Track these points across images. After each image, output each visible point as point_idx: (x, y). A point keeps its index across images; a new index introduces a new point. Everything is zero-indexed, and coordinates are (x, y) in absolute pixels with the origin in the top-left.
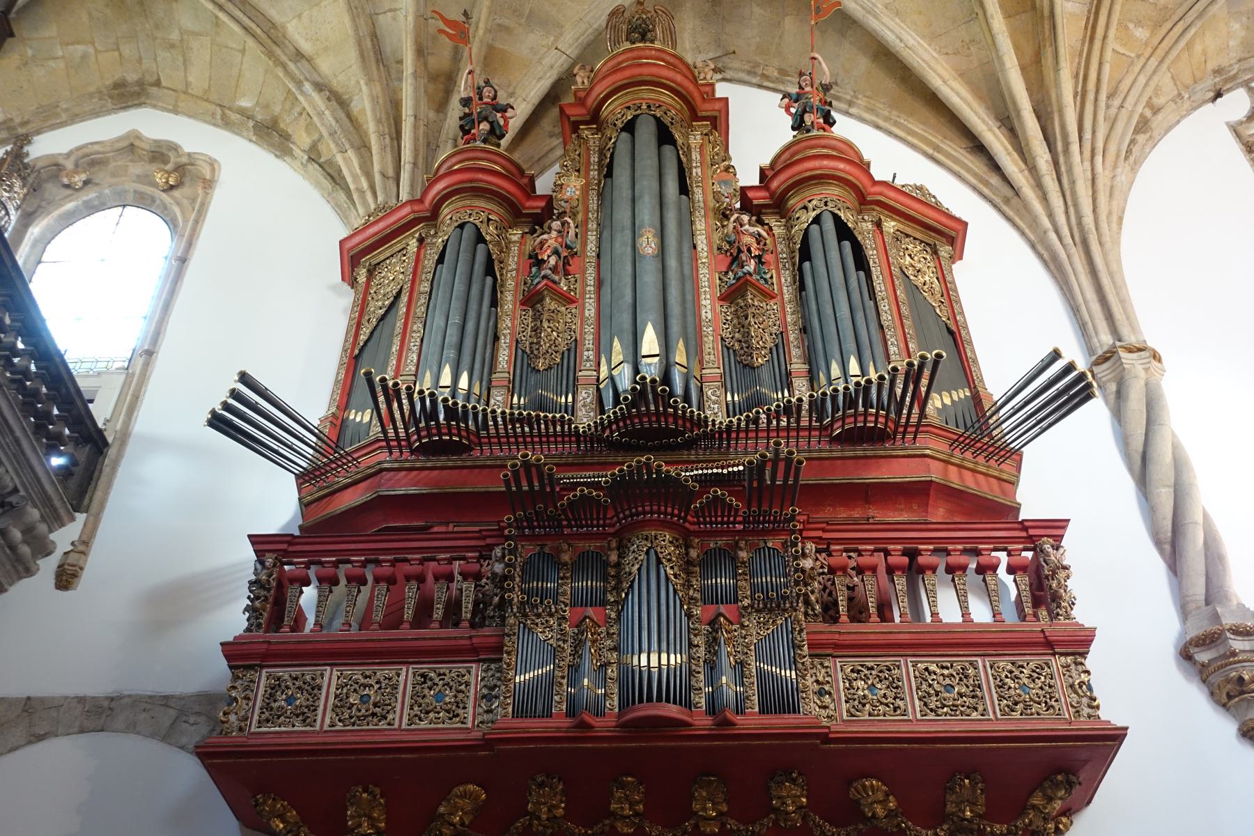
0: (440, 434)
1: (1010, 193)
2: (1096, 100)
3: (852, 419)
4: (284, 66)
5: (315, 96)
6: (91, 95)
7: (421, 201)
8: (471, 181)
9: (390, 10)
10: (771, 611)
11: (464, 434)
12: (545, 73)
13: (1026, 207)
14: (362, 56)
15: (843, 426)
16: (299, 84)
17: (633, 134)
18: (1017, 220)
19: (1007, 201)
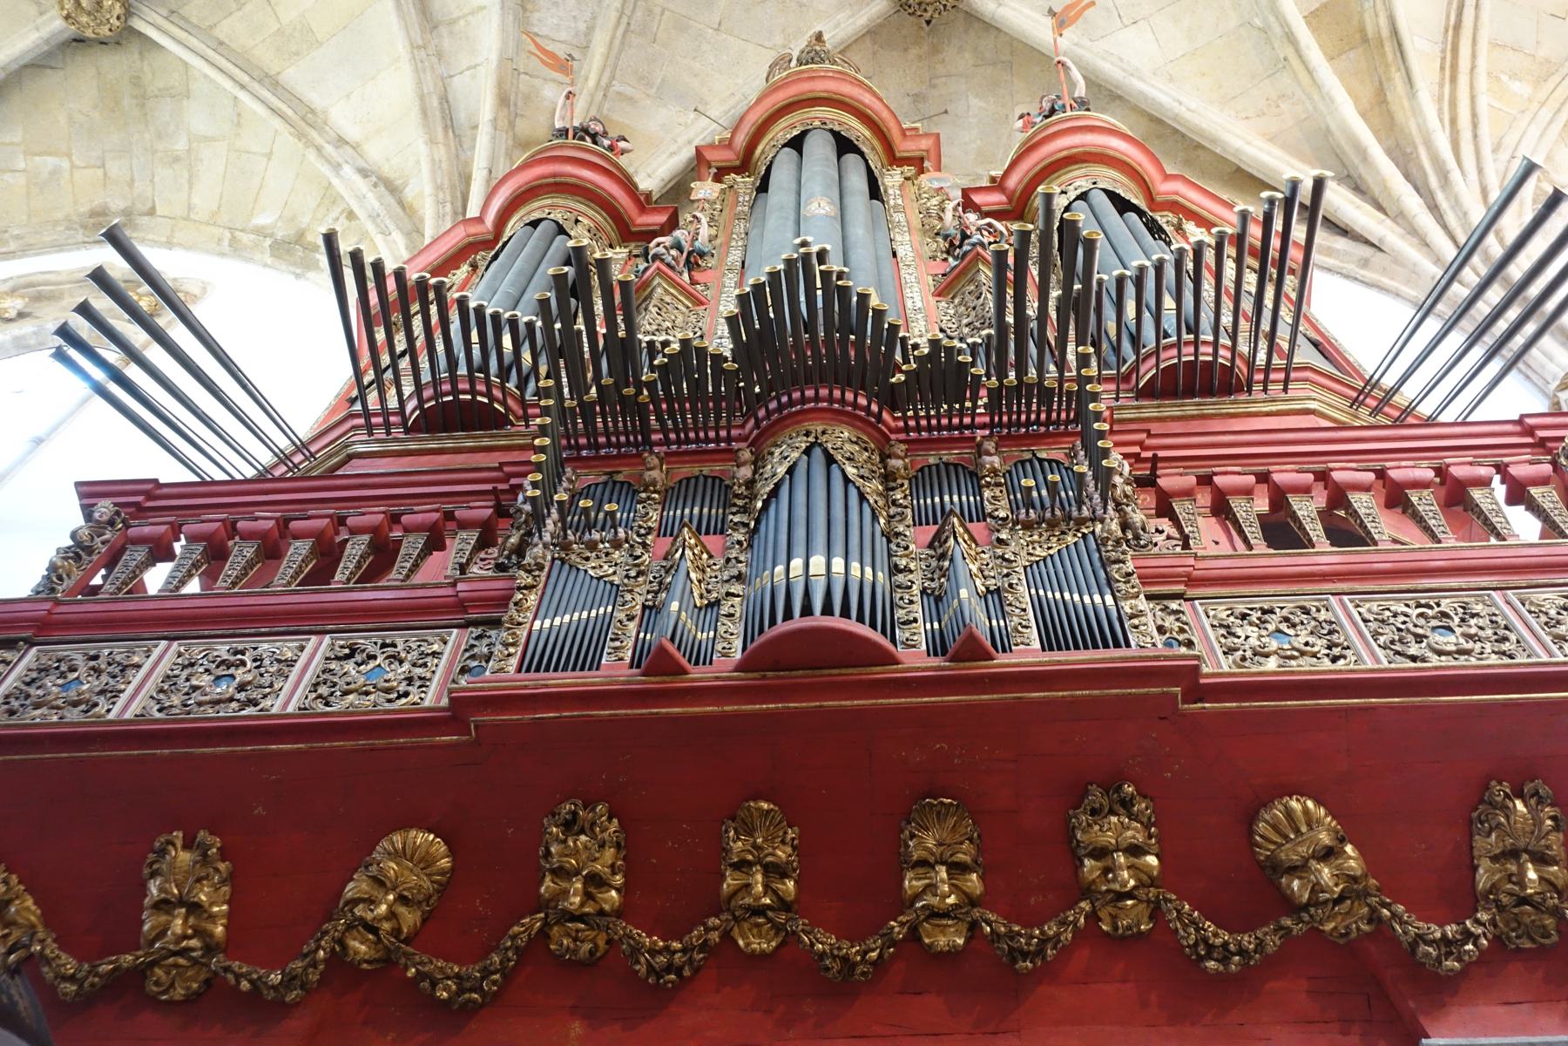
0: (455, 391)
1: (1366, 251)
2: (1475, 136)
3: (1174, 352)
4: (319, 149)
5: (357, 178)
6: (56, 223)
7: (480, 220)
8: (554, 176)
9: (468, 69)
10: (1052, 525)
11: (497, 393)
12: (680, 149)
13: (1397, 260)
14: (424, 112)
15: (1157, 365)
16: (337, 167)
17: (800, 152)
18: (1385, 281)
19: (1365, 263)
